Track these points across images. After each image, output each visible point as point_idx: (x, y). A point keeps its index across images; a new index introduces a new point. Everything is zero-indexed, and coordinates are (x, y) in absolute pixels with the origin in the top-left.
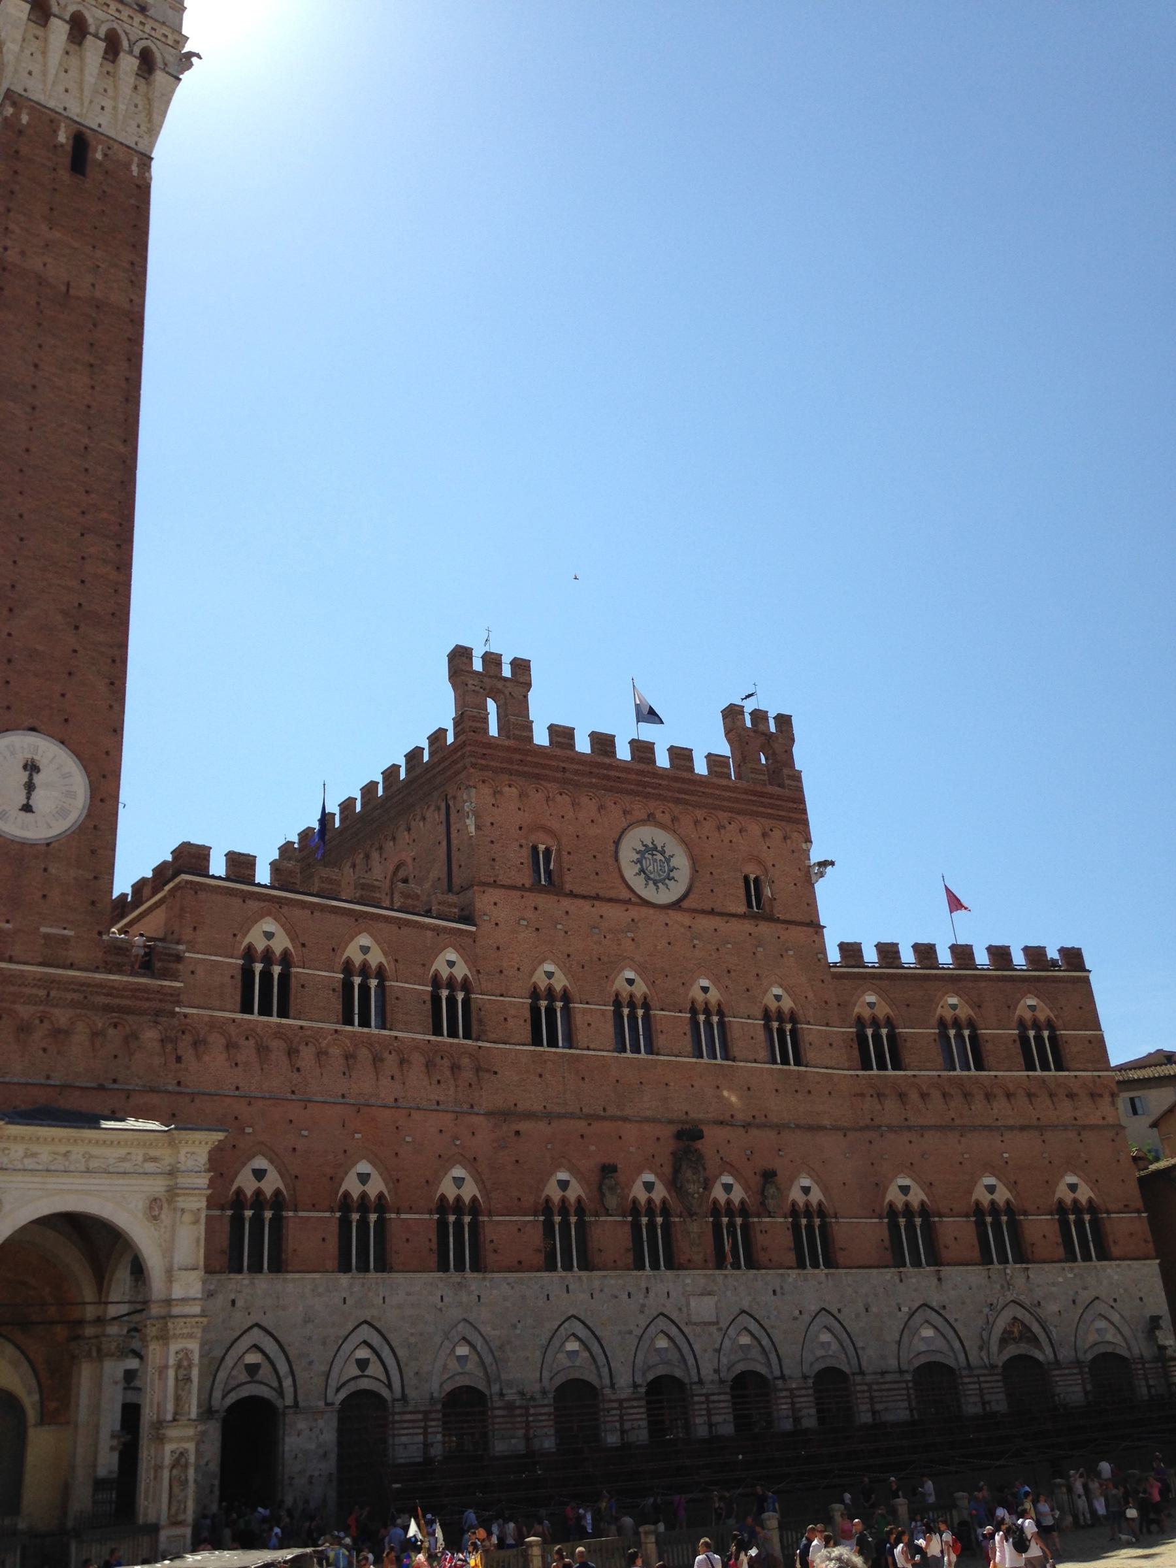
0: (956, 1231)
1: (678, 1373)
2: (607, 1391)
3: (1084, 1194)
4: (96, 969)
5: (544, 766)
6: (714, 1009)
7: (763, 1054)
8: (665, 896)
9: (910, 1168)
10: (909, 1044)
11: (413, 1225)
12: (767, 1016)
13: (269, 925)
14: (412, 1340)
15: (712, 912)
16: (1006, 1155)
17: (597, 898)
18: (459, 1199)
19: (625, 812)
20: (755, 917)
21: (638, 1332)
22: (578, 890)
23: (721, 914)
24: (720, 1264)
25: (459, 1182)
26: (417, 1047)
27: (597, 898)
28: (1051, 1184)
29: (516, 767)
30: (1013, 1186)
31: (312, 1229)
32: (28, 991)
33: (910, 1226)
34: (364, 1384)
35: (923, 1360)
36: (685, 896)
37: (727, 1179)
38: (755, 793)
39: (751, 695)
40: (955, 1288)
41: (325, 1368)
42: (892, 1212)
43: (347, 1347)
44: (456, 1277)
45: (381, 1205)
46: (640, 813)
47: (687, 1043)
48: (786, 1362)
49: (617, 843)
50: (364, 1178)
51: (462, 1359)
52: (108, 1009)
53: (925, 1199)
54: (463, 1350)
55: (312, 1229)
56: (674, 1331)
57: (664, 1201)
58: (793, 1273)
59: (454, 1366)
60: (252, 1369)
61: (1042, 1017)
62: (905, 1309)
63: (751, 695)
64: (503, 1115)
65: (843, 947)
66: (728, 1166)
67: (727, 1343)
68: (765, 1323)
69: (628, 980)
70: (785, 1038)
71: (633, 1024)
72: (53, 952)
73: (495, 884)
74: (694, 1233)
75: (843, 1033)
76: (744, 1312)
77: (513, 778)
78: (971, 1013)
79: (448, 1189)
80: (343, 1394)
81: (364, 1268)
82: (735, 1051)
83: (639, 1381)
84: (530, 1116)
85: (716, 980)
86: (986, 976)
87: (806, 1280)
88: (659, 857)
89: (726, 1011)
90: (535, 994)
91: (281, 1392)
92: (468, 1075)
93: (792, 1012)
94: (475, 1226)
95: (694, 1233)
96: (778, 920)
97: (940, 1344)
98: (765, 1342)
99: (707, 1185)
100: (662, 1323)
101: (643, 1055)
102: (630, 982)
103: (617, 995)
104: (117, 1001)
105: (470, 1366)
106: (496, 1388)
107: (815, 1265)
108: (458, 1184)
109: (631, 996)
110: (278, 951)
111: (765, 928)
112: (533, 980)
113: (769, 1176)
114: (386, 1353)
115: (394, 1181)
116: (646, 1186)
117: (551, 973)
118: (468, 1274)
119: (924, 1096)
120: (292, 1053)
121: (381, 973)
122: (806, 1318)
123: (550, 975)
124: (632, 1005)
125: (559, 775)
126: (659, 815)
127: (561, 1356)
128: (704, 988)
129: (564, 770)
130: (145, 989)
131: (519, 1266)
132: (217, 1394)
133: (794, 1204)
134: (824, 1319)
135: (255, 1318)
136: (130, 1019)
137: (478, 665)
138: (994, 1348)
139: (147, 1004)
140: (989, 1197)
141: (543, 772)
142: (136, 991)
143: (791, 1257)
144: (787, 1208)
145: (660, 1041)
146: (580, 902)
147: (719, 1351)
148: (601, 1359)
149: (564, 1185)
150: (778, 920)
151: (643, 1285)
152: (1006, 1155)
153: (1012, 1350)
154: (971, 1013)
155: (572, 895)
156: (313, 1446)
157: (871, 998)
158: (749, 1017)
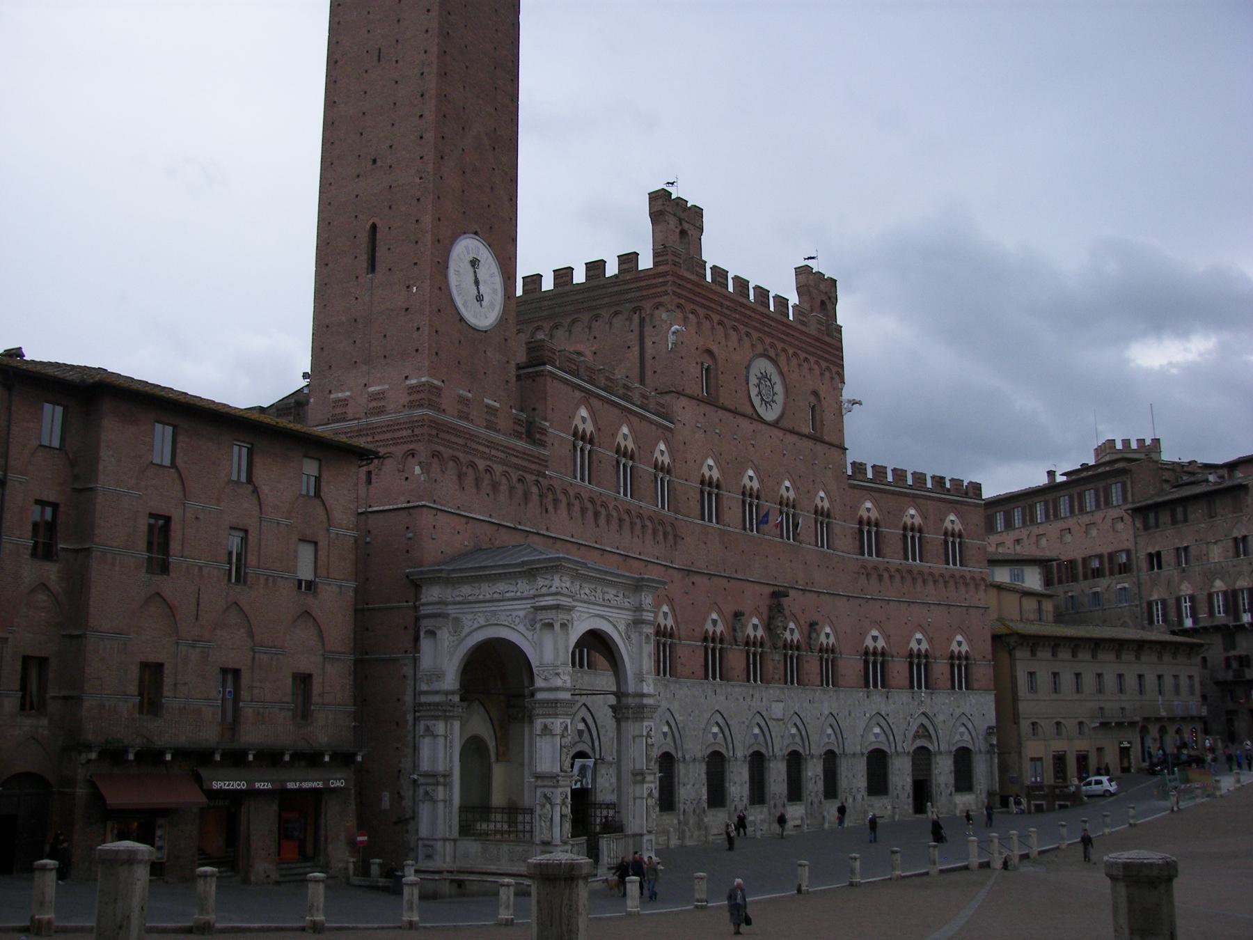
0: (898, 669)
5: (712, 300)
8: (770, 415)
9: (878, 624)
15: (793, 432)
19: (753, 346)
22: (728, 404)
30: (930, 640)
32: (482, 448)
36: (781, 416)
38: (818, 340)
42: (866, 653)
46: (760, 349)
48: (813, 746)
49: (748, 368)
52: (517, 467)
65: (854, 464)
77: (697, 308)
92: (671, 537)
97: (882, 738)
98: (804, 733)
100: (758, 719)
106: (680, 755)
111: (819, 447)
113: (813, 625)
117: (711, 469)
119: (891, 577)
120: (596, 515)
129: (722, 305)
148: (729, 739)
153: (919, 743)
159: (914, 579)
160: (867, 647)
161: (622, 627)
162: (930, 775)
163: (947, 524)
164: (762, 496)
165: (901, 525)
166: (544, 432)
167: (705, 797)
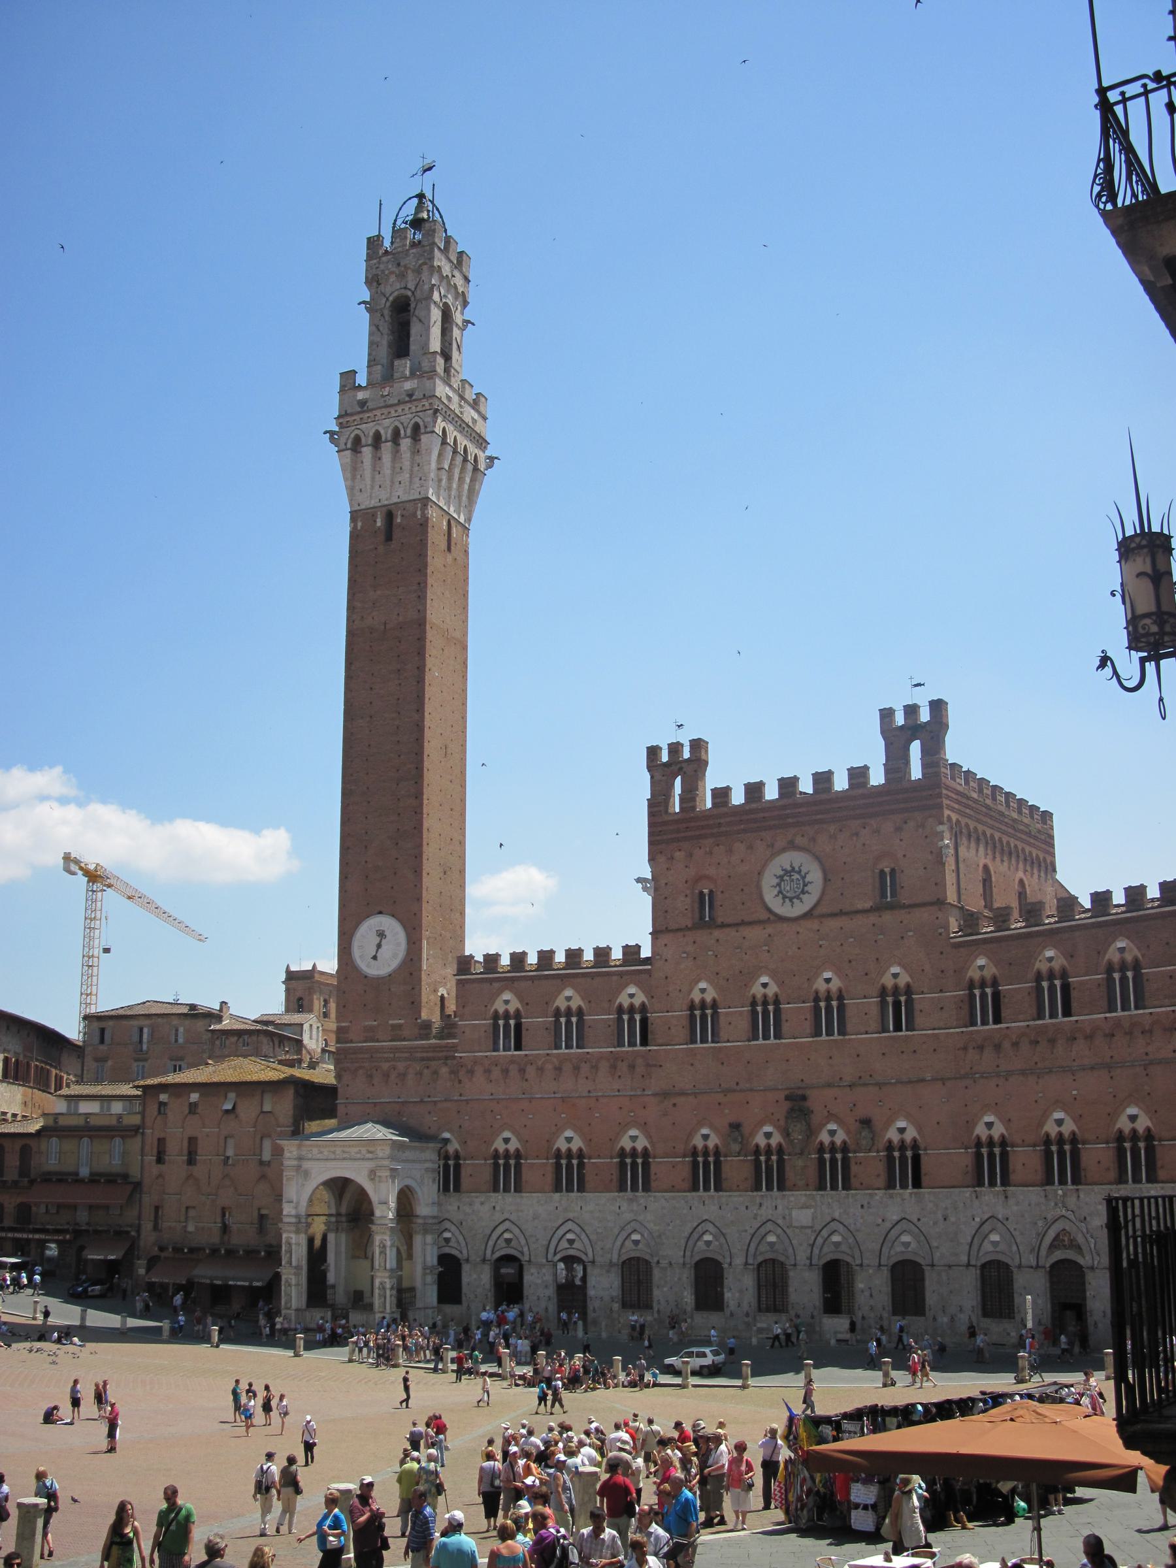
0: (1025, 1160)
1: (782, 1259)
2: (725, 1266)
3: (1143, 1123)
4: (416, 1039)
5: (703, 827)
6: (834, 994)
7: (874, 1025)
8: (799, 909)
10: (1006, 1000)
11: (601, 1164)
12: (883, 992)
13: (507, 996)
14: (600, 1231)
16: (1075, 1092)
17: (743, 923)
18: (634, 1149)
20: (879, 908)
21: (752, 1231)
23: (847, 914)
24: (821, 1187)
25: (634, 1138)
26: (601, 1057)
27: (743, 923)
28: (1113, 1116)
29: (683, 835)
30: (1078, 1119)
31: (537, 1169)
33: (991, 1155)
34: (572, 1252)
35: (988, 1258)
37: (832, 1126)
39: (916, 685)
40: (1017, 1204)
41: (545, 1243)
42: (978, 1144)
43: (560, 1232)
44: (629, 1194)
45: (581, 1155)
47: (808, 1027)
50: (569, 1140)
51: (636, 1242)
53: (1005, 1132)
54: (635, 1237)
55: (537, 1169)
56: (779, 1231)
57: (780, 1145)
58: (880, 1193)
59: (628, 1244)
60: (508, 1241)
61: (1129, 957)
62: (978, 1219)
63: (916, 685)
64: (664, 1095)
66: (831, 1116)
67: (820, 1240)
68: (852, 1228)
69: (764, 985)
70: (898, 1008)
71: (766, 1017)
72: (396, 1033)
73: (668, 930)
74: (800, 1166)
75: (955, 996)
76: (834, 1220)
78: (1065, 963)
79: (627, 1144)
80: (558, 1257)
81: (569, 1189)
82: (849, 1027)
83: (750, 1261)
84: (683, 1094)
85: (838, 972)
86: (1118, 920)
87: (891, 1197)
88: (796, 876)
89: (845, 994)
90: (692, 1007)
91: (522, 1253)
93: (908, 986)
94: (646, 1165)
95: (800, 1166)
96: (904, 907)
99: (811, 1132)
101: (772, 1040)
102: (765, 985)
103: (754, 997)
104: (425, 1055)
105: (640, 1246)
106: (655, 1259)
107: (904, 1186)
108: (634, 1139)
109: (765, 996)
110: (512, 1010)
111: (888, 917)
112: (692, 996)
113: (866, 1122)
114: (583, 1236)
115: (588, 1141)
116: (767, 1135)
118: (640, 1194)
119: (1015, 1045)
120: (522, 1071)
121: (580, 1013)
122: (888, 1225)
123: (703, 991)
124: (765, 1003)
125: (715, 831)
126: (799, 840)
127: (700, 1243)
128: (828, 980)
130: (440, 1046)
131: (673, 1189)
132: (489, 1252)
133: (890, 1141)
134: (904, 1225)
135: (506, 1215)
136: (433, 1063)
137: (665, 758)
138: (1043, 1252)
139: (441, 1054)
140: (1057, 1129)
141: (703, 832)
142: (434, 1048)
143: (881, 1181)
144: (881, 1144)
145: (785, 1027)
146: (727, 930)
147: (813, 1246)
148: (726, 1246)
149: (706, 1137)
150: (904, 907)
151: (758, 1200)
152: (1075, 1092)
153: (1059, 1255)
154: (1065, 963)
155: (723, 926)
156: (539, 1281)
157: (981, 961)
158: (865, 997)
159: (1052, 1041)
160: (978, 1138)
161: (365, 1173)
162: (1084, 1299)
163: (1112, 955)
164: (781, 999)
165: (1031, 975)
166: (454, 1025)
167: (688, 1298)
